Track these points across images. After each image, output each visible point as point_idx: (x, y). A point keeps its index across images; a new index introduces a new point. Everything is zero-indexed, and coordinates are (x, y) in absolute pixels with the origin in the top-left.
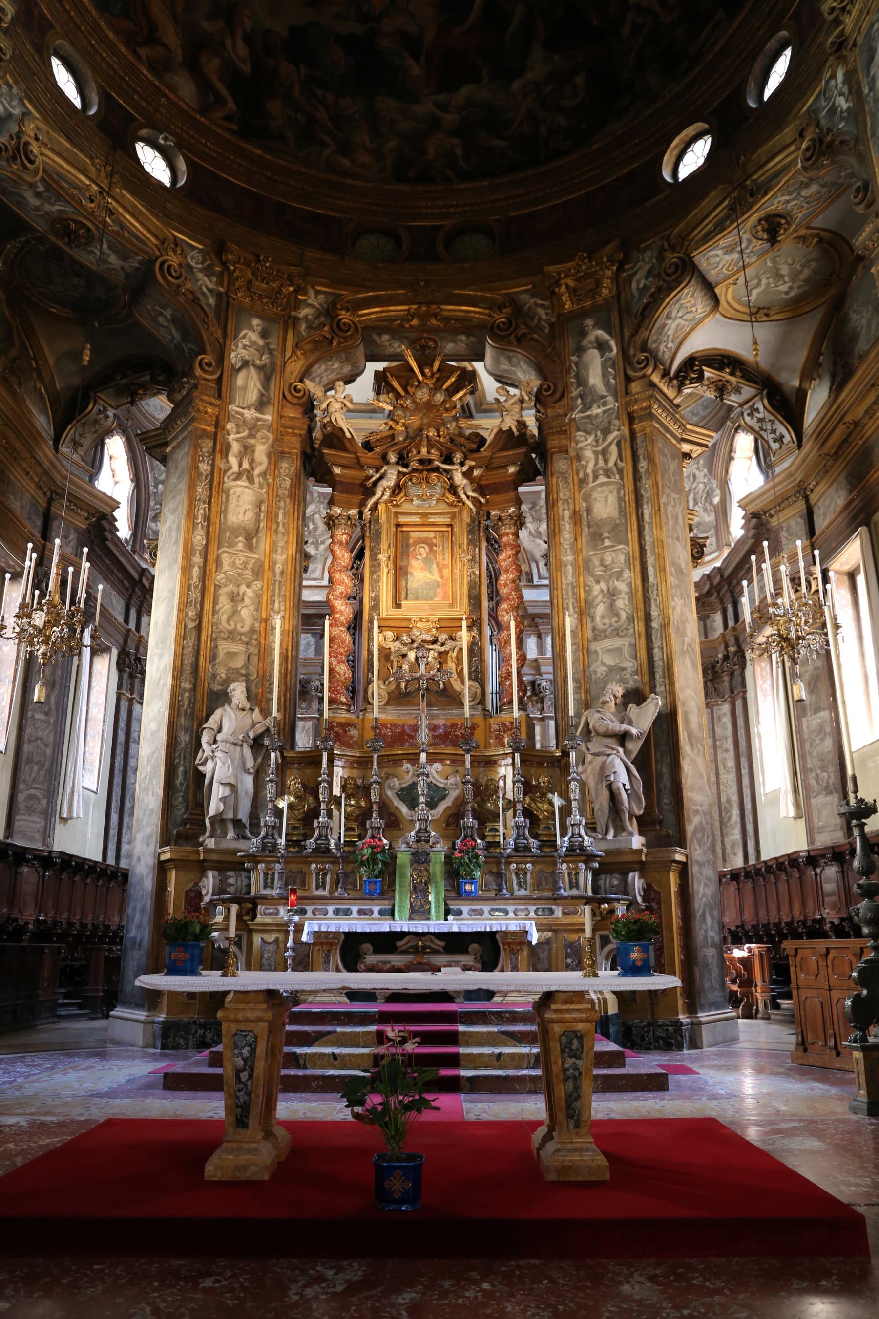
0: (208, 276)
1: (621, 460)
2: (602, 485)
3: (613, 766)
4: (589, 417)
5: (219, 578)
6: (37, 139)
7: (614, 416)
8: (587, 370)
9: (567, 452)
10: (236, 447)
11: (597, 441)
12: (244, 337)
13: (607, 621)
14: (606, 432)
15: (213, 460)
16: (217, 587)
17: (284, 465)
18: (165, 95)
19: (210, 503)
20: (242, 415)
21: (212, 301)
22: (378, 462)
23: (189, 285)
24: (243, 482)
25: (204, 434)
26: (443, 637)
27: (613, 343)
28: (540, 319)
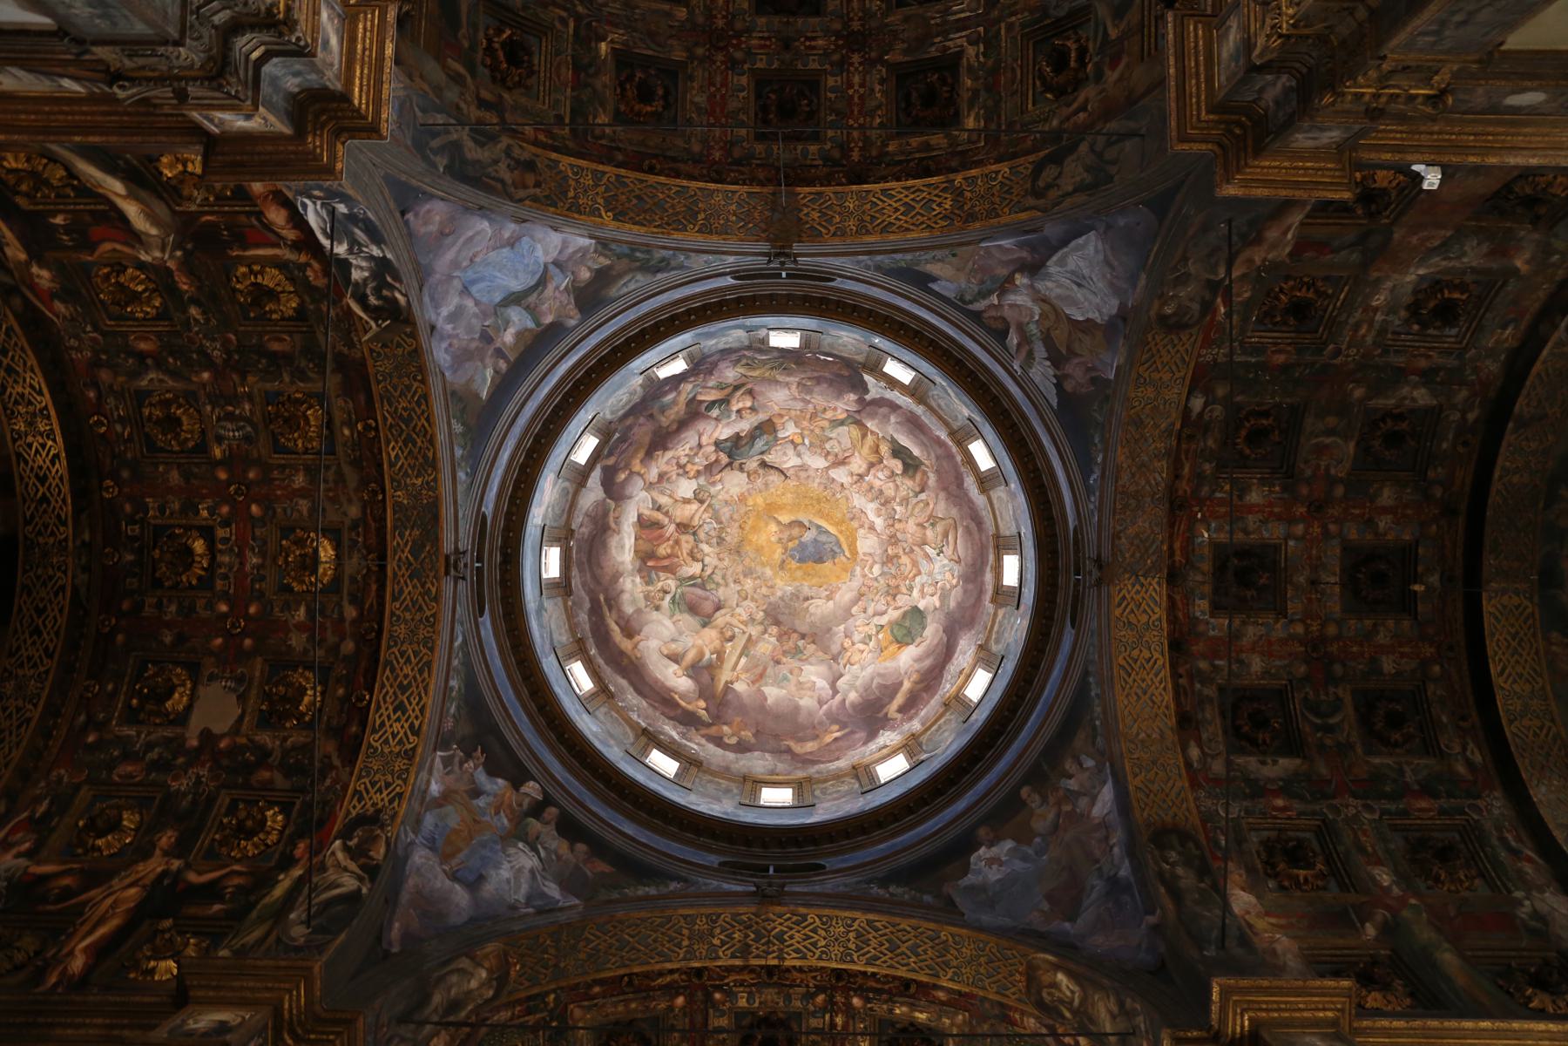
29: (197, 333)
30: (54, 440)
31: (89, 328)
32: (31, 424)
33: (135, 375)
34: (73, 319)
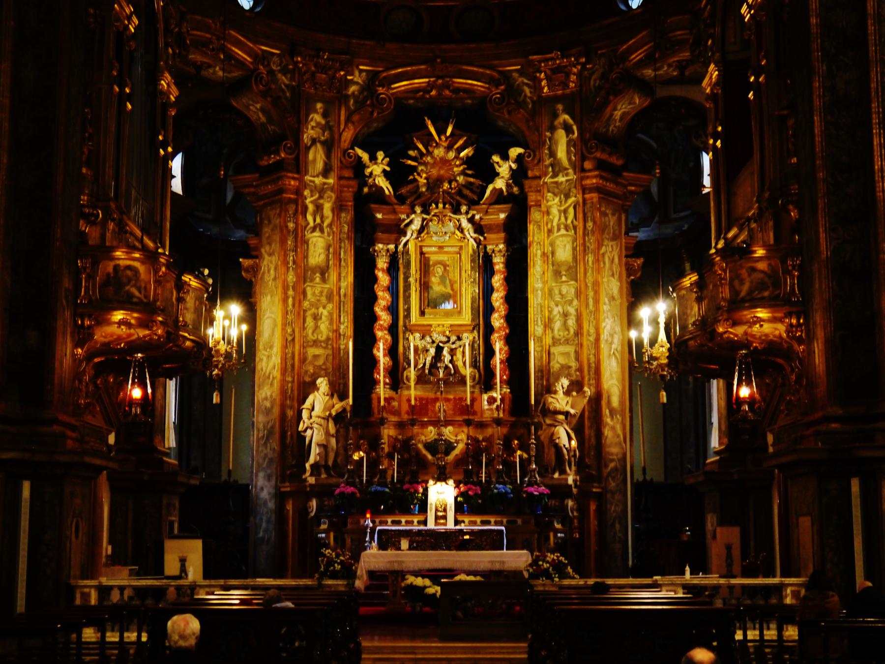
1: (576, 220)
2: (563, 235)
3: (558, 433)
4: (556, 183)
5: (305, 305)
7: (573, 185)
8: (556, 144)
9: (540, 206)
10: (311, 207)
11: (561, 202)
12: (312, 120)
13: (561, 333)
14: (567, 196)
15: (297, 219)
16: (305, 311)
17: (343, 215)
19: (296, 251)
20: (313, 182)
22: (408, 211)
24: (317, 233)
25: (290, 201)
26: (453, 338)
27: (575, 128)
28: (526, 95)
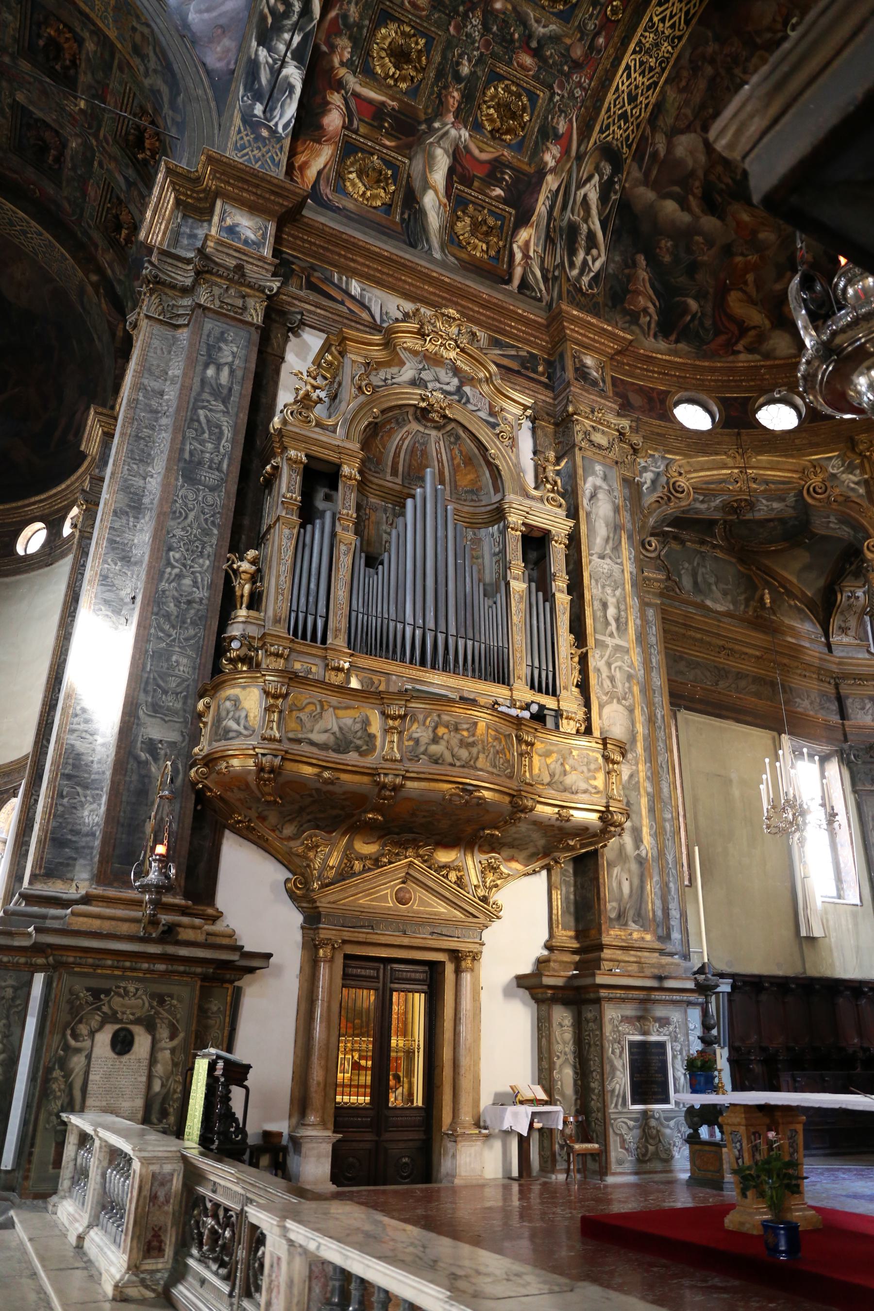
0: (851, 473)
6: (680, 474)
18: (763, 366)
21: (862, 491)
23: (837, 491)
29: (478, 48)
30: (651, 19)
31: (557, 98)
32: (657, 45)
33: (555, 39)
34: (561, 111)
